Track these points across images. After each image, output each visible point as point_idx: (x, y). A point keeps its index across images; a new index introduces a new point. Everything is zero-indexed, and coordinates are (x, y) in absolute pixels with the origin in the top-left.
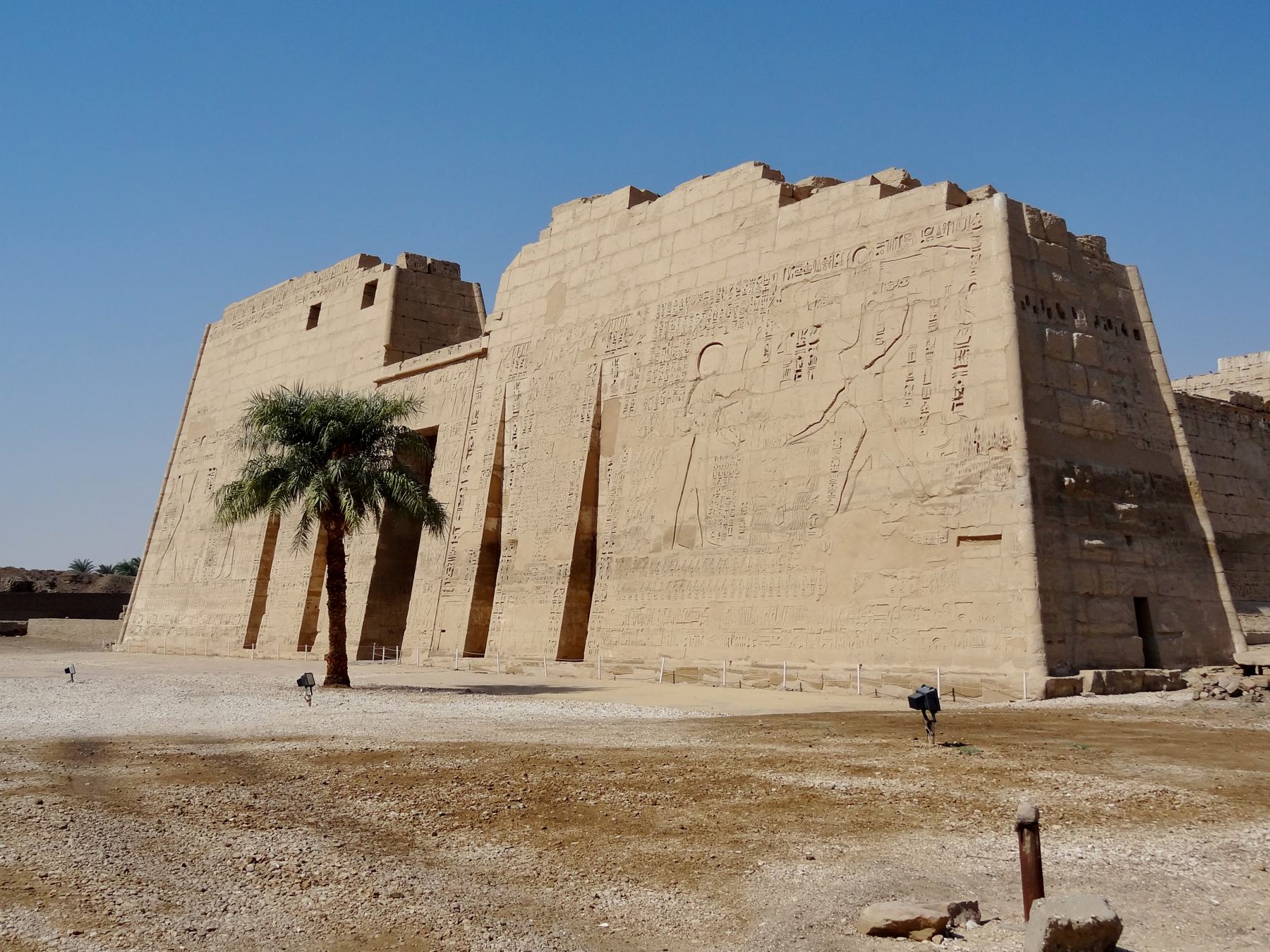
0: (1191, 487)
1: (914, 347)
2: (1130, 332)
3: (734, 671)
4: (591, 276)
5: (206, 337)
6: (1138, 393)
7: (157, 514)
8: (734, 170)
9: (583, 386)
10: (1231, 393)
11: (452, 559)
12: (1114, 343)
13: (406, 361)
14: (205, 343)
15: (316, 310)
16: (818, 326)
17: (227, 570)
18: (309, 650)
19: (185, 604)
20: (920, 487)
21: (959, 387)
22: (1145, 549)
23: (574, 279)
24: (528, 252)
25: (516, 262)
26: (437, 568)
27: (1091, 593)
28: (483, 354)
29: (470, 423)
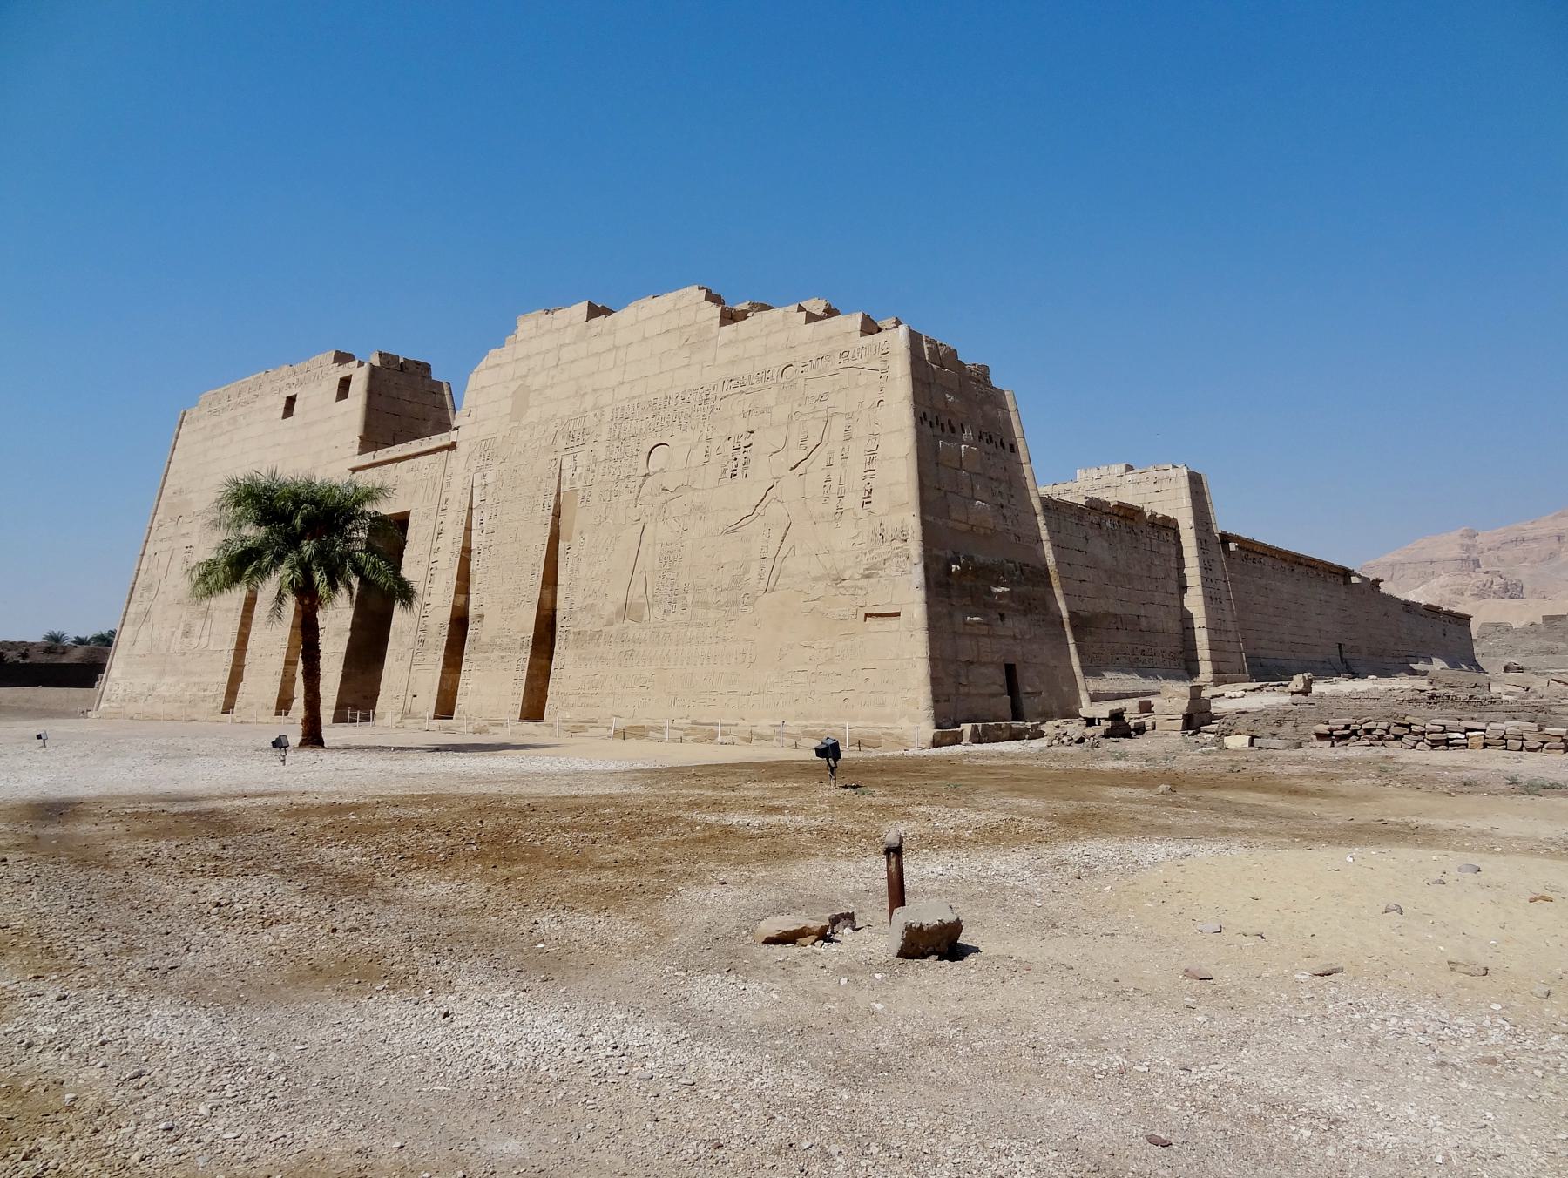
0: (1052, 574)
1: (831, 453)
2: (1007, 446)
3: (676, 728)
4: (553, 378)
5: (182, 422)
6: (1012, 496)
7: (133, 589)
8: (680, 292)
9: (544, 478)
10: (1086, 498)
11: (423, 631)
12: (994, 454)
13: (379, 451)
14: (180, 428)
15: (291, 401)
16: (752, 432)
17: (204, 641)
19: (162, 674)
20: (835, 572)
21: (868, 487)
22: (1014, 625)
23: (536, 382)
24: (494, 356)
26: (409, 640)
27: (971, 660)
28: (452, 447)
29: (440, 511)
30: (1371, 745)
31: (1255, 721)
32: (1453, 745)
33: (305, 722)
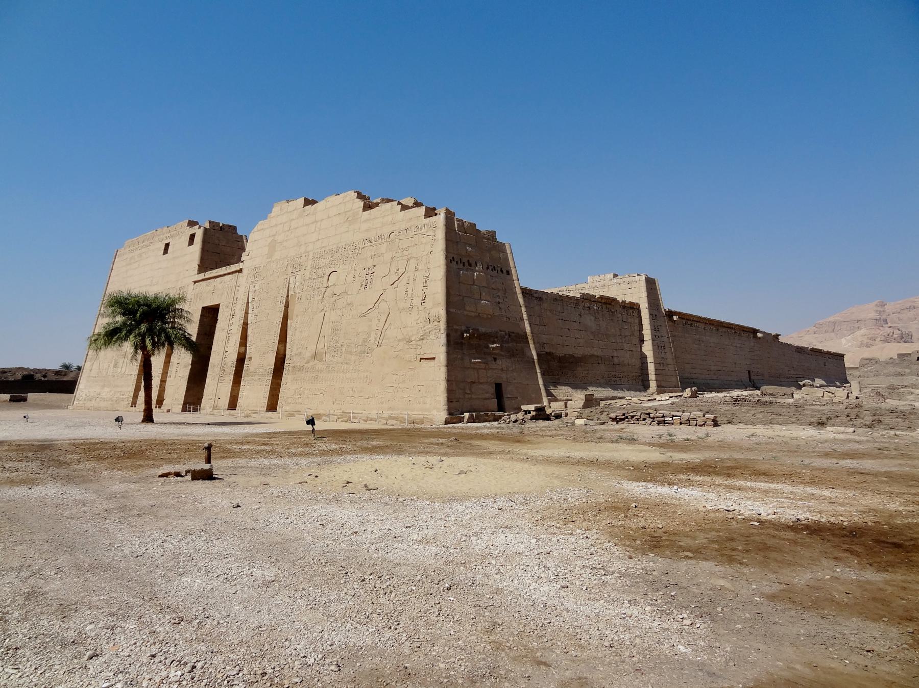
0: (529, 337)
1: (409, 277)
2: (505, 272)
3: (334, 415)
4: (287, 237)
5: (116, 256)
6: (507, 298)
8: (346, 194)
9: (282, 287)
10: (581, 293)
11: (224, 365)
12: (496, 277)
13: (207, 273)
14: (115, 259)
15: (167, 245)
16: (375, 266)
17: (123, 370)
18: (135, 407)
19: (103, 386)
20: (408, 337)
21: (424, 295)
22: (502, 363)
23: (279, 238)
24: (261, 224)
25: (255, 229)
26: (217, 370)
27: (474, 381)
28: (240, 271)
30: (634, 423)
31: (591, 412)
32: (667, 423)
33: (145, 410)
